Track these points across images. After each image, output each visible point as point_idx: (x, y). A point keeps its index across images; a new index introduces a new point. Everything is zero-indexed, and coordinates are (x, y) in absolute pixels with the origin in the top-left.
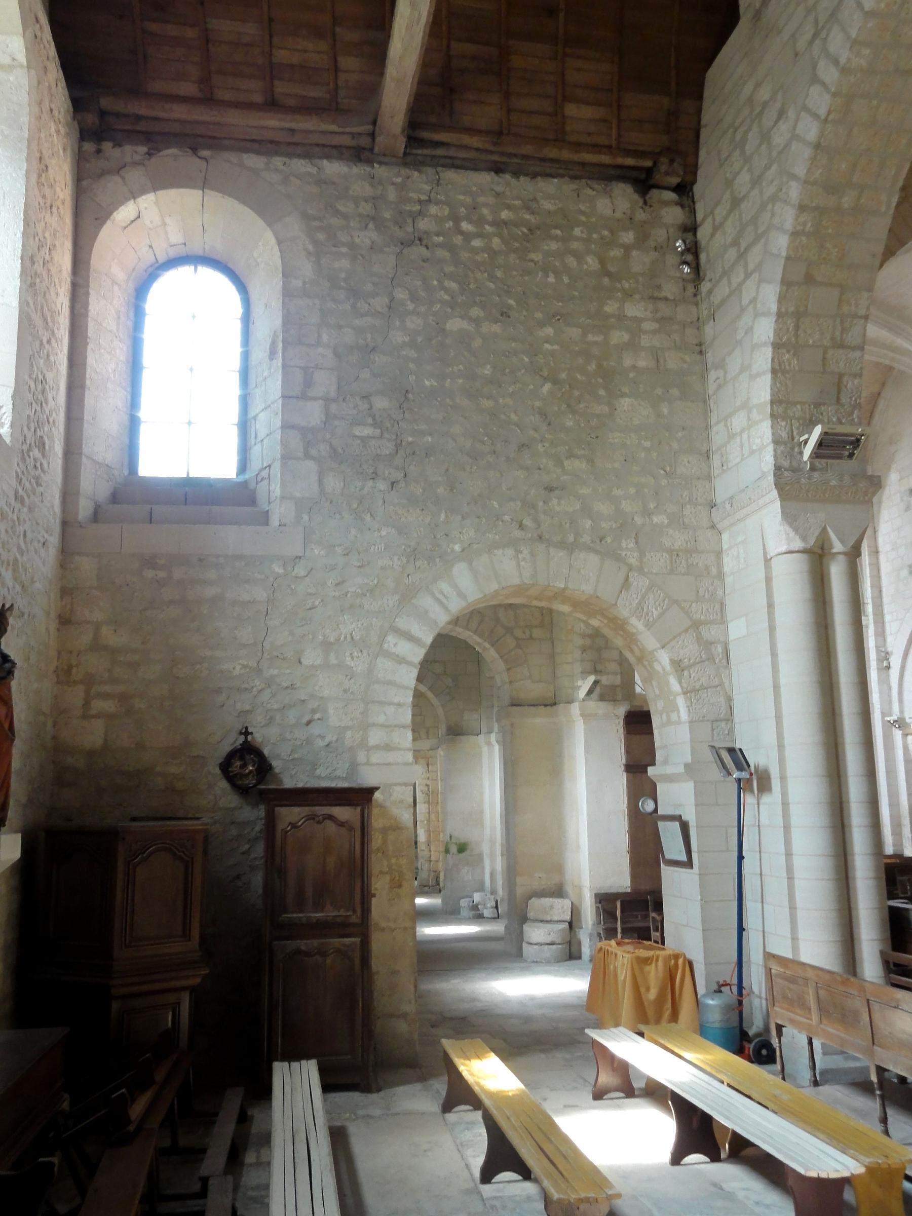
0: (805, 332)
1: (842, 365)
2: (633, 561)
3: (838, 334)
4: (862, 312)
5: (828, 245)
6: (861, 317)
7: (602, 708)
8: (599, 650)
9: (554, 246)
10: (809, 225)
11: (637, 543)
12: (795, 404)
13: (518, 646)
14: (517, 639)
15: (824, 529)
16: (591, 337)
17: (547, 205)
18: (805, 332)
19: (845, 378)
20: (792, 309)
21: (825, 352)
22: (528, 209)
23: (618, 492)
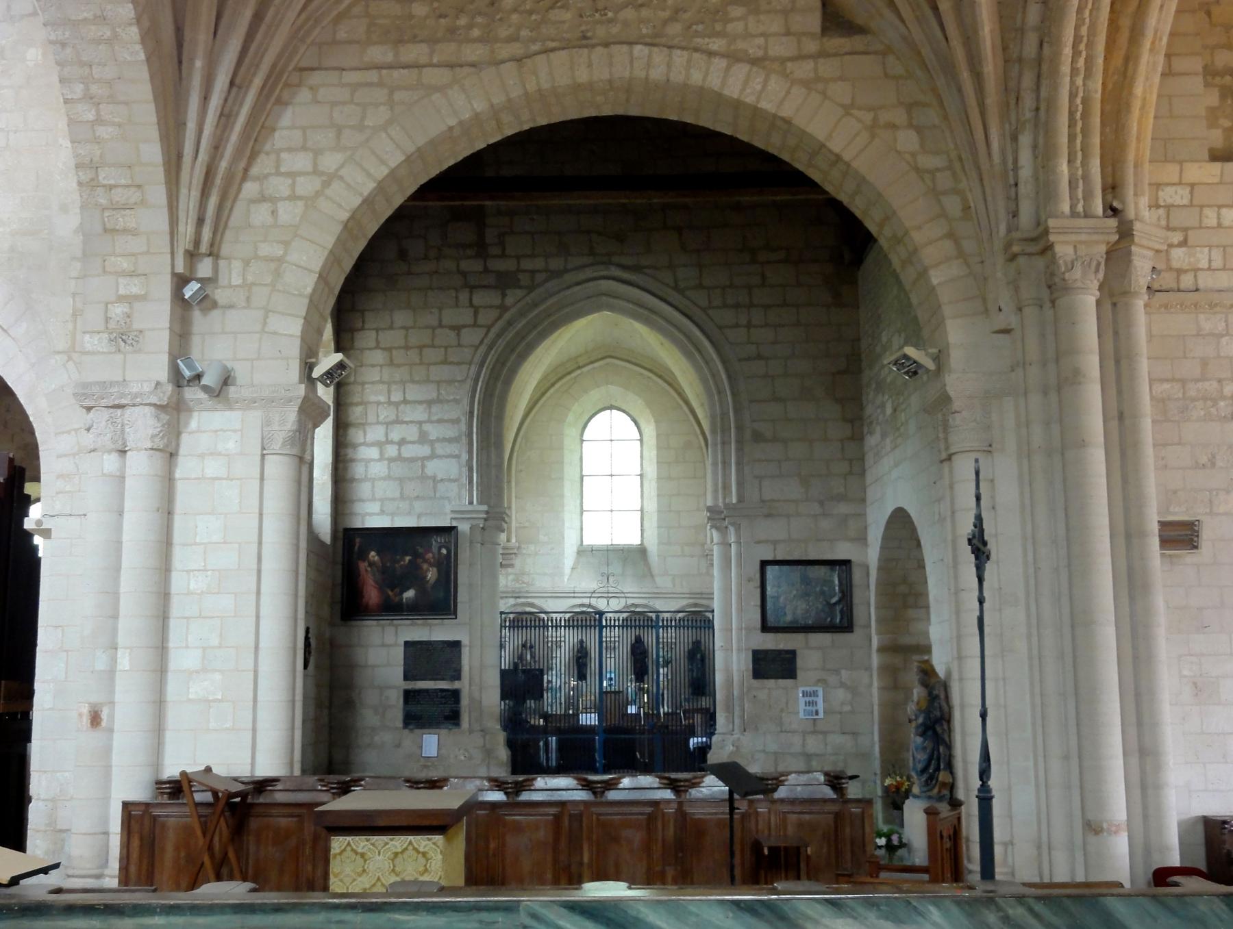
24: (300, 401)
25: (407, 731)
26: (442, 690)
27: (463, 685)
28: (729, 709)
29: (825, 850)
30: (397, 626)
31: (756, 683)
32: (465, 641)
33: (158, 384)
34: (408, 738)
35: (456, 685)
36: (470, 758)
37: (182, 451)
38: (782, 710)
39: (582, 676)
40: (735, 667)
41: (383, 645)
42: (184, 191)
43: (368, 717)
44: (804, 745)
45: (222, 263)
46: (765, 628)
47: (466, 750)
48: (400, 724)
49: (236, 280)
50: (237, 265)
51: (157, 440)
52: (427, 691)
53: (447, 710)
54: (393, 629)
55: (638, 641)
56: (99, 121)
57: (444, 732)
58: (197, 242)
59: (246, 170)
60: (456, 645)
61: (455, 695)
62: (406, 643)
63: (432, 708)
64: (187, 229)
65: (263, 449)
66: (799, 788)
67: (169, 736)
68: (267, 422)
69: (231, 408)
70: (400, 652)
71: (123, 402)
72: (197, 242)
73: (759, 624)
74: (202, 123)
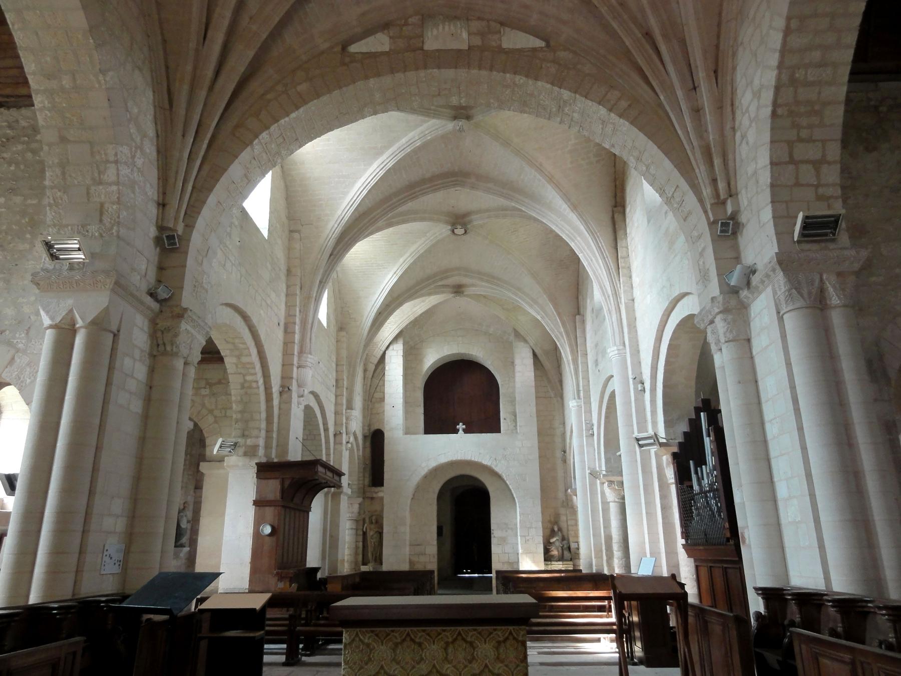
0: (70, 176)
1: (103, 196)
2: (20, 346)
3: (96, 175)
4: (112, 158)
5: (68, 115)
6: (111, 162)
7: (246, 460)
8: (247, 422)
9: (20, 147)
10: (46, 102)
11: (27, 334)
12: (67, 226)
13: (216, 422)
14: (215, 417)
15: (71, 311)
16: (29, 202)
17: (23, 123)
18: (70, 176)
19: (106, 206)
20: (56, 161)
21: (88, 189)
22: (10, 127)
23: (20, 300)
24: (778, 267)
33: (713, 299)
37: (753, 335)
42: (697, 171)
45: (739, 196)
49: (746, 203)
50: (743, 192)
51: (728, 335)
56: (648, 167)
58: (717, 194)
59: (733, 129)
64: (707, 192)
65: (778, 313)
67: (788, 552)
68: (775, 293)
69: (760, 293)
71: (710, 317)
72: (717, 194)
74: (684, 126)
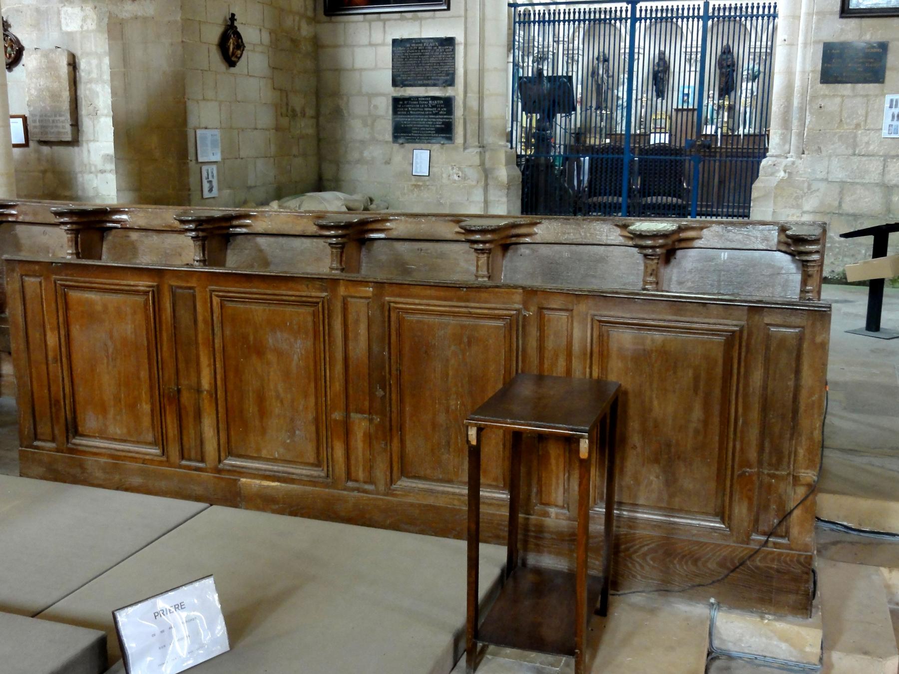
25: (396, 146)
26: (434, 98)
27: (457, 92)
28: (786, 124)
29: (697, 413)
30: (385, 21)
31: (825, 89)
32: (460, 38)
34: (398, 153)
35: (449, 92)
36: (465, 178)
38: (858, 126)
39: (660, 93)
40: (798, 68)
41: (371, 45)
43: (357, 130)
44: (883, 174)
46: (846, 12)
47: (460, 168)
48: (389, 137)
52: (417, 98)
53: (439, 121)
54: (381, 24)
55: (727, 51)
57: (436, 147)
60: (449, 42)
61: (448, 103)
62: (395, 41)
63: (424, 119)
66: (725, 255)
70: (389, 49)
73: (837, 7)
